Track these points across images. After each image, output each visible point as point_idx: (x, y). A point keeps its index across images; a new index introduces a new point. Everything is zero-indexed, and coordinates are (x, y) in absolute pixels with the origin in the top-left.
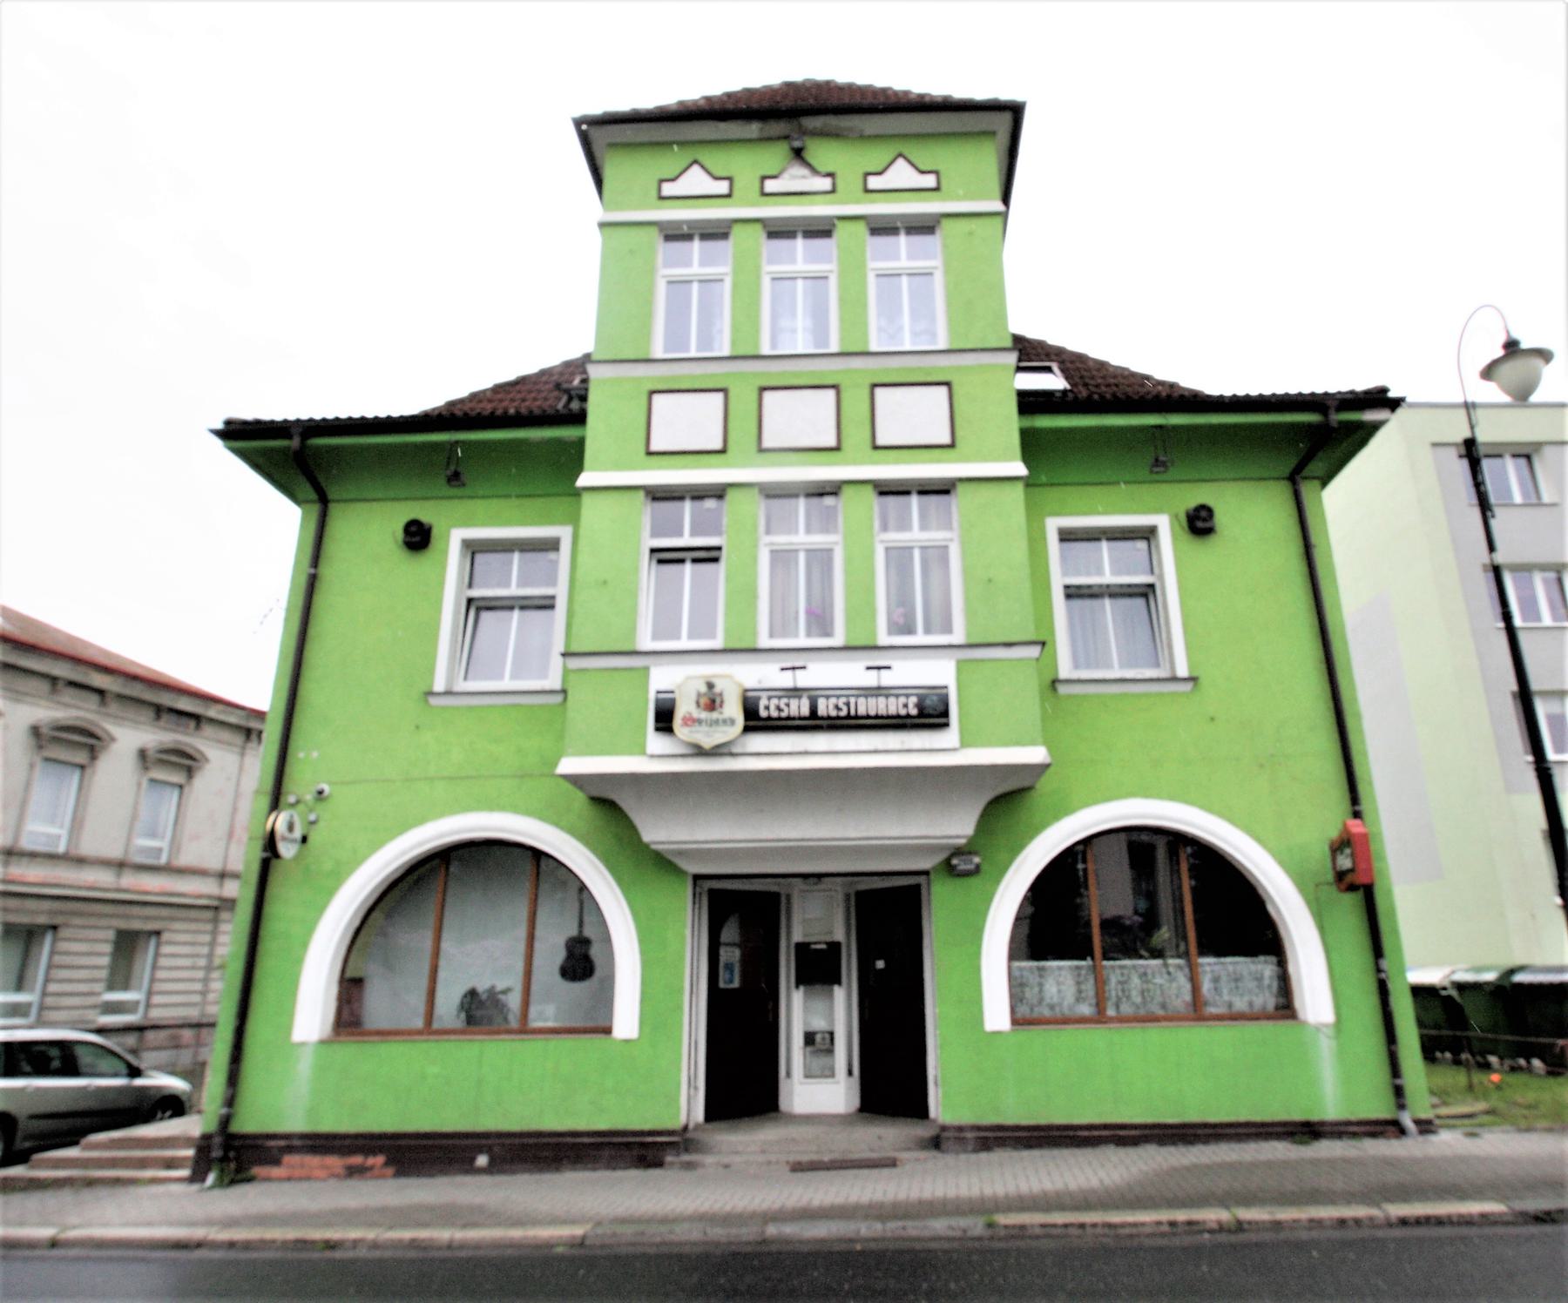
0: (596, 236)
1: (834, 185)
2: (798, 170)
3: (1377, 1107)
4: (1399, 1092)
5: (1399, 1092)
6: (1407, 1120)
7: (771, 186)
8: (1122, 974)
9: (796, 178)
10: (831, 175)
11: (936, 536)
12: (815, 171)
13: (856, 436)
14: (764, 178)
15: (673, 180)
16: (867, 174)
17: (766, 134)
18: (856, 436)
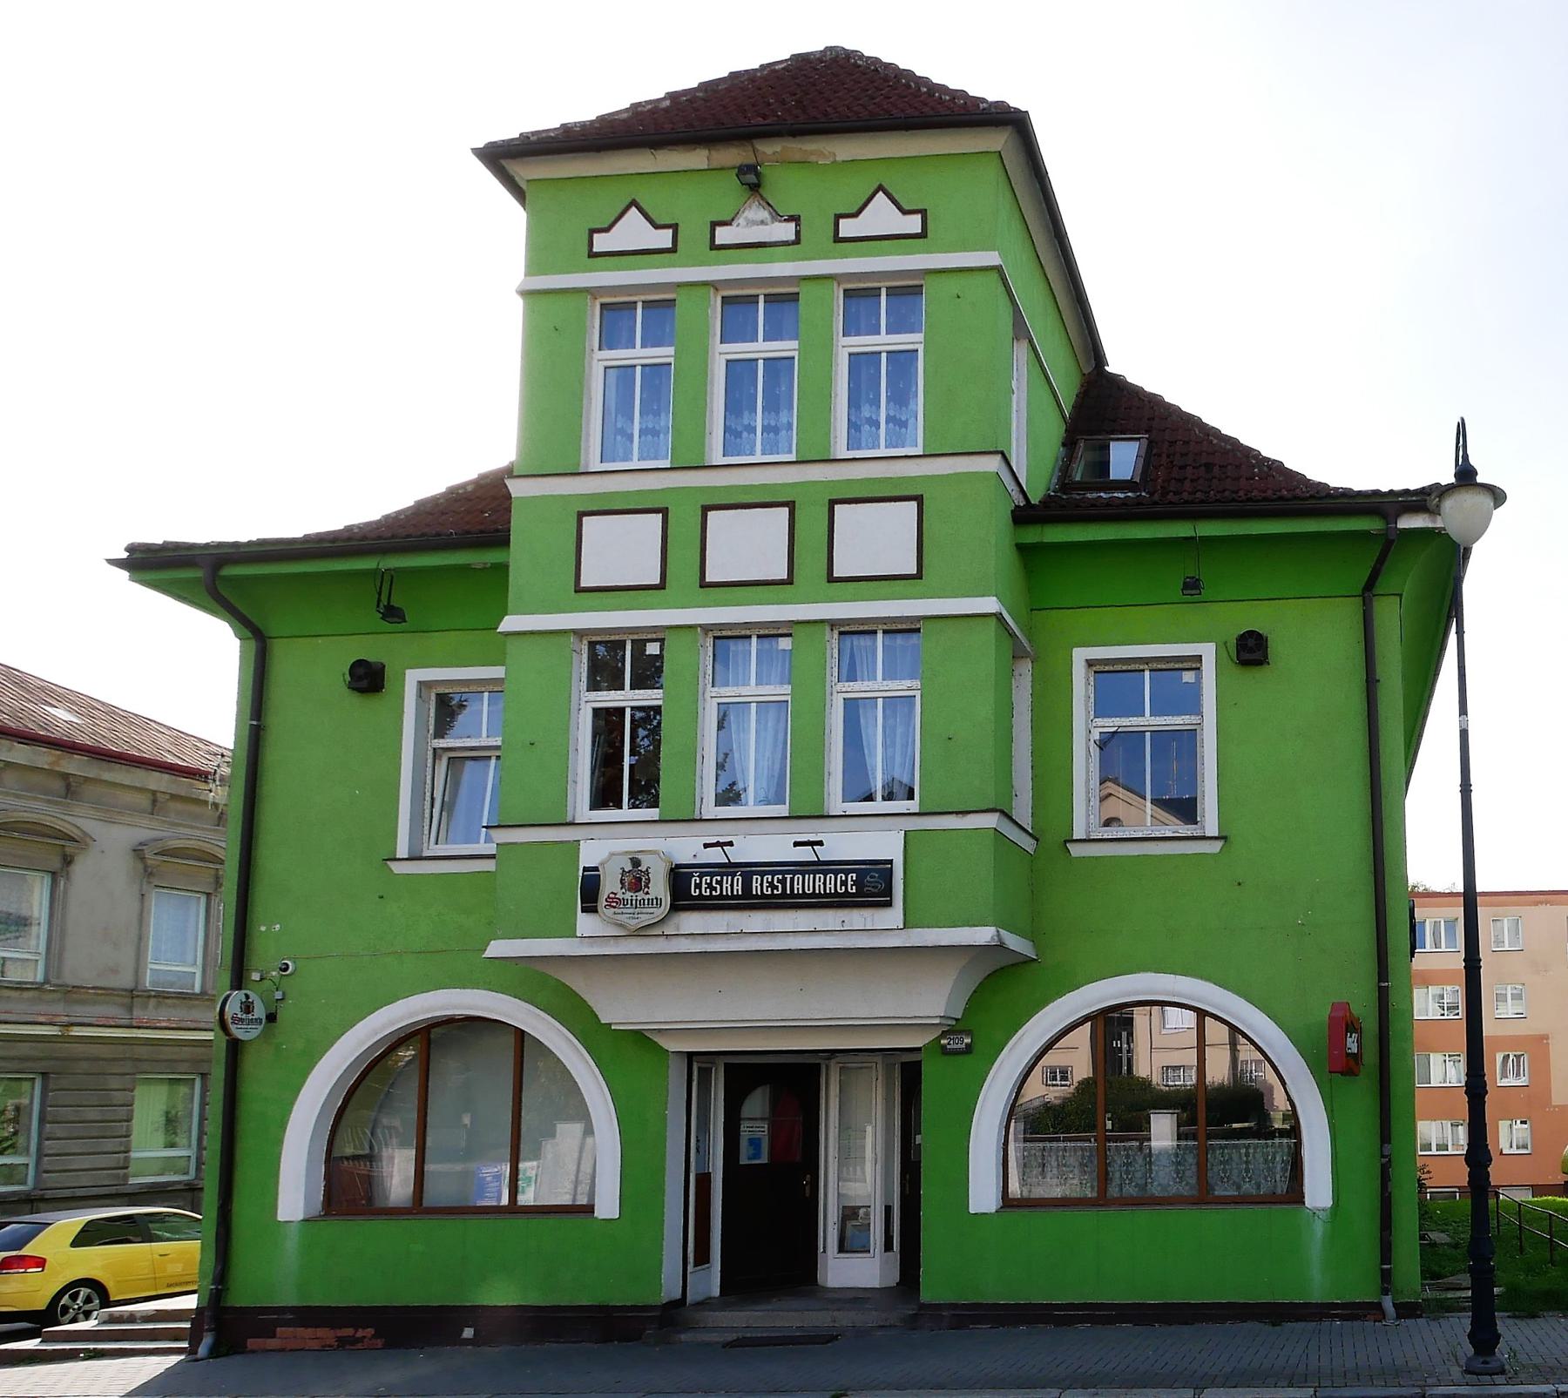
0: (518, 304)
1: (798, 233)
2: (756, 212)
3: (1362, 1290)
4: (1386, 1276)
5: (1386, 1276)
6: (1388, 1303)
7: (724, 235)
8: (1128, 1156)
9: (753, 225)
10: (795, 219)
11: (900, 687)
12: (777, 216)
13: (810, 566)
14: (714, 225)
15: (607, 230)
16: (838, 217)
17: (715, 165)
18: (810, 566)
